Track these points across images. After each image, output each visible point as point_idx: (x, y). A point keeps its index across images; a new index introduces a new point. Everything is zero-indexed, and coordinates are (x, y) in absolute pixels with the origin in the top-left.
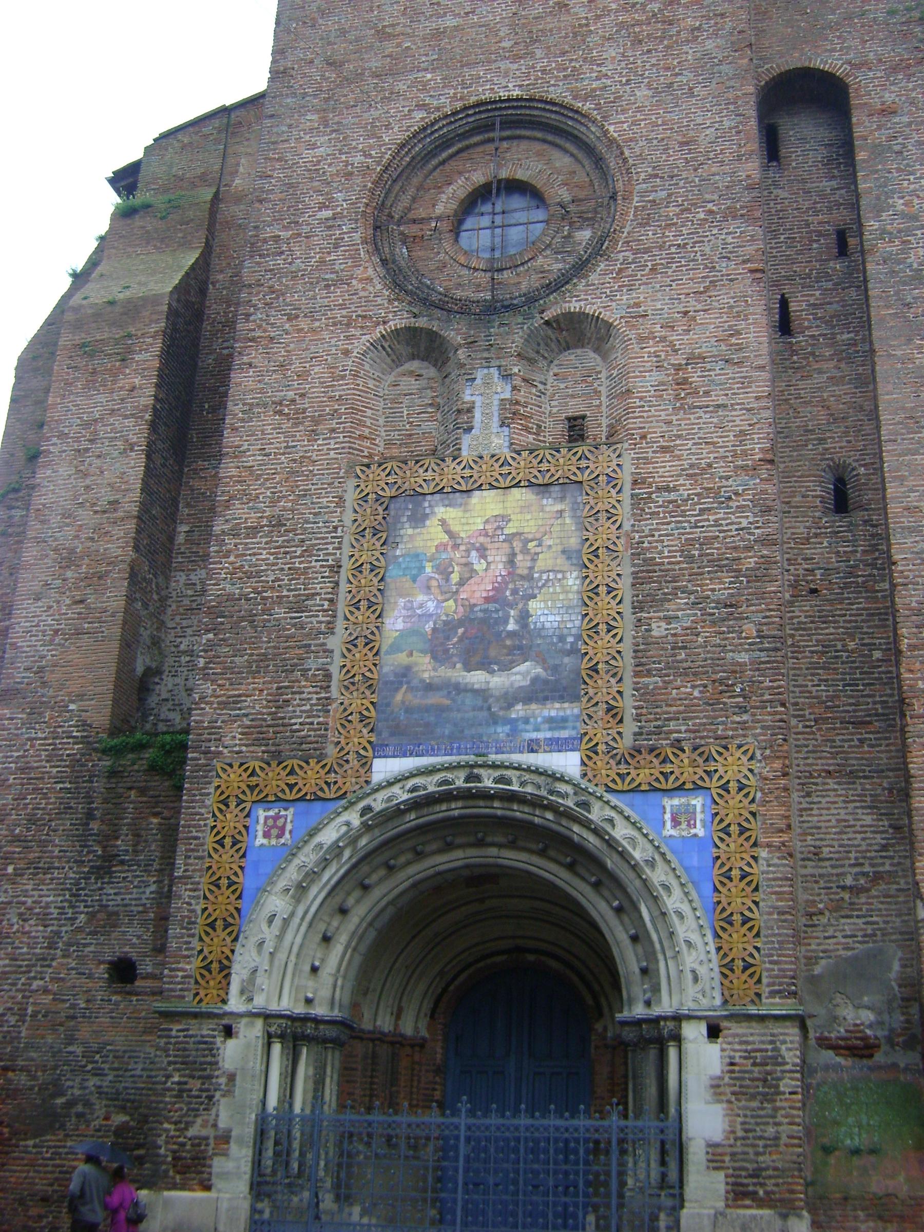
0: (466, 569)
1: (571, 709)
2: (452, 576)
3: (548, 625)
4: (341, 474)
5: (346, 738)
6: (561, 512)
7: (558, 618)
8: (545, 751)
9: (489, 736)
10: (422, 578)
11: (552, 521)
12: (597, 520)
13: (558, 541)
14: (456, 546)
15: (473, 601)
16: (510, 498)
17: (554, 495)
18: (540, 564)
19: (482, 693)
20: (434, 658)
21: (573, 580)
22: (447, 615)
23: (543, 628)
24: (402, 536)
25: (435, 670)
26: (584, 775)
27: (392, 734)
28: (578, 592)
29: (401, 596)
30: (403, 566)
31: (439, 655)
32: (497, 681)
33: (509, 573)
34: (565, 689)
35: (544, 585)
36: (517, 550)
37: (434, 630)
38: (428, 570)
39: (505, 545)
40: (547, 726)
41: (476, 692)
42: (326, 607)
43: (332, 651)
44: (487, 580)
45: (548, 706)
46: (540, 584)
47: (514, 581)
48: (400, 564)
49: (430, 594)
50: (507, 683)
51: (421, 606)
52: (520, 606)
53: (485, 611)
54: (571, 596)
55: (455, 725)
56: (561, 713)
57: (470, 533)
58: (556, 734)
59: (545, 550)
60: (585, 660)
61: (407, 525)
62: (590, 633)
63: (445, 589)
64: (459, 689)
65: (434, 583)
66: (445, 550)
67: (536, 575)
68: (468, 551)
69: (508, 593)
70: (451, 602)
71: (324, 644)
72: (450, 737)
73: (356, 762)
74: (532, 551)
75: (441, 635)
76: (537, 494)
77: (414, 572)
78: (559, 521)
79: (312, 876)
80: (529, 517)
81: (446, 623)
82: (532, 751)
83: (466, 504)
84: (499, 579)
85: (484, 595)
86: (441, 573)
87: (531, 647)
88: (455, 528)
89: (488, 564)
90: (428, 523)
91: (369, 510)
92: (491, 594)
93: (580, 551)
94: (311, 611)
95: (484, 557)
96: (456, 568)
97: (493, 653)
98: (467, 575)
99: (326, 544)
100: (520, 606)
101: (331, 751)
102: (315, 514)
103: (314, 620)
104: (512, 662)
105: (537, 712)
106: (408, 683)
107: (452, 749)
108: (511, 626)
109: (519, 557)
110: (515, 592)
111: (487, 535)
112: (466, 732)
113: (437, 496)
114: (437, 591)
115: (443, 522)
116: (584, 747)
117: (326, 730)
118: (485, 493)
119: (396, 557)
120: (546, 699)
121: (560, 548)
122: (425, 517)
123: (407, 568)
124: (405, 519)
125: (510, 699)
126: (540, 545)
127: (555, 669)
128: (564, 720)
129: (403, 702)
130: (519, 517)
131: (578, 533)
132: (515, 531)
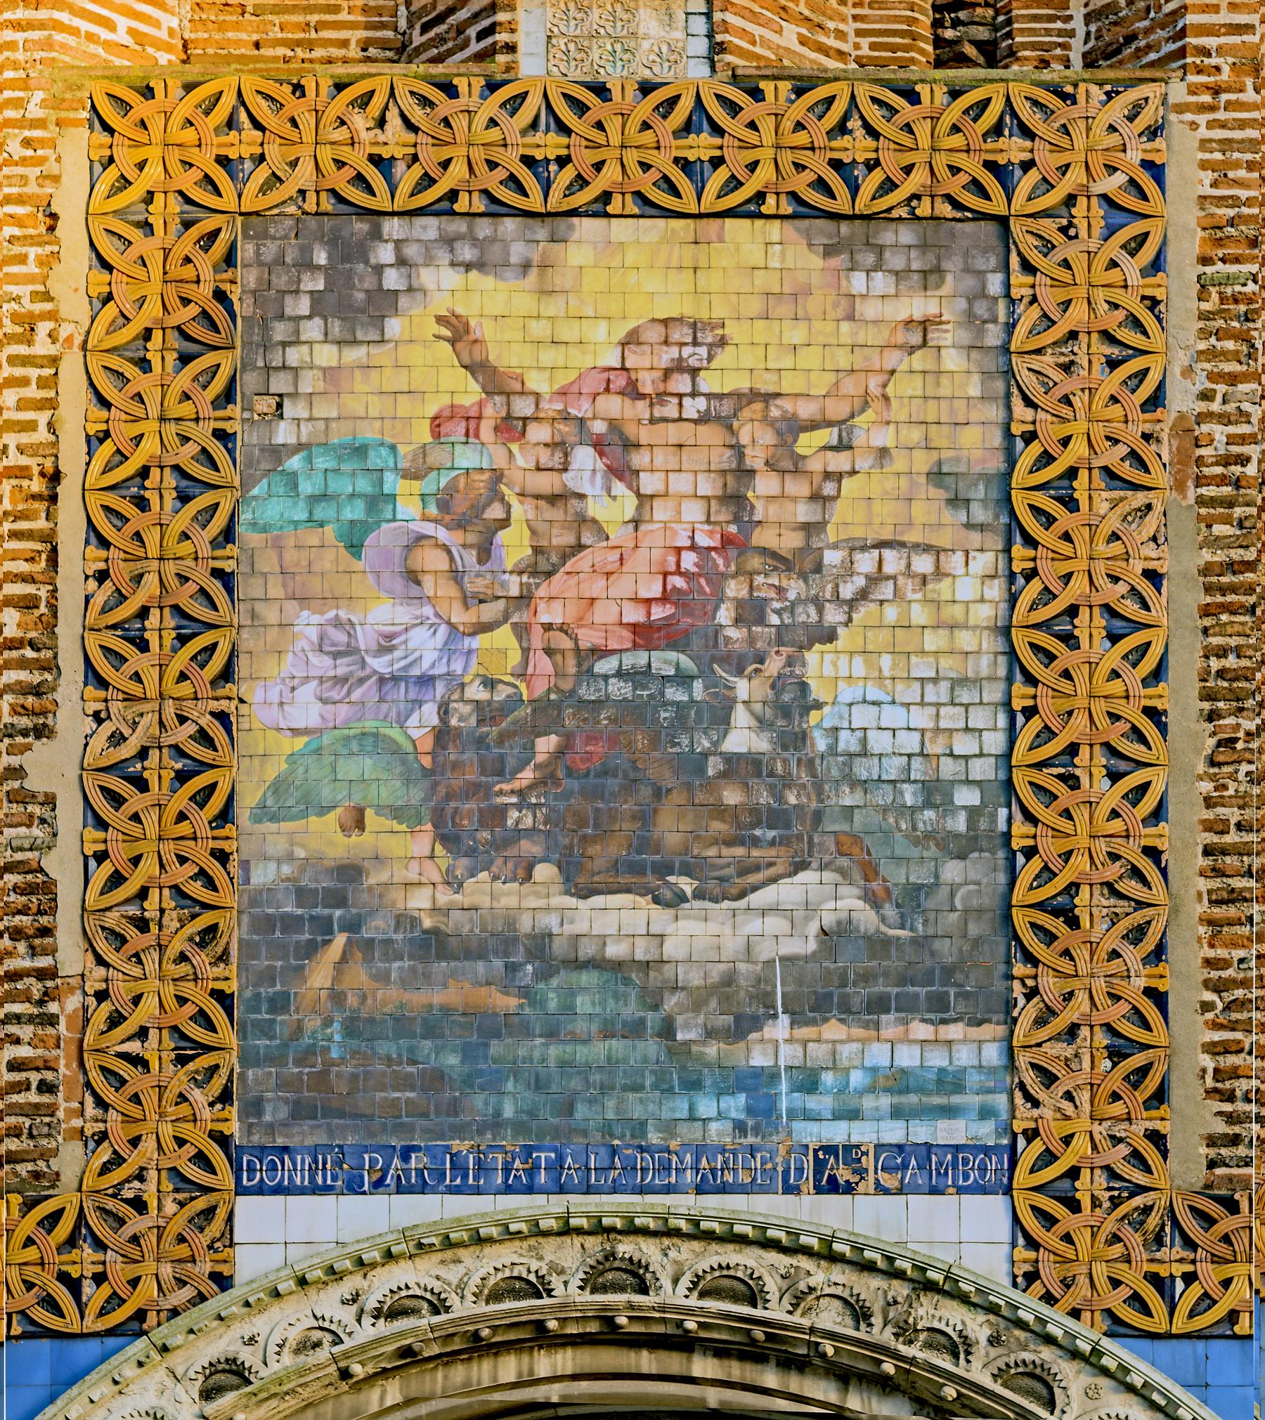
3: (879, 742)
7: (921, 718)
10: (384, 538)
11: (892, 359)
14: (511, 428)
15: (588, 638)
18: (846, 517)
21: (974, 584)
29: (303, 600)
33: (727, 541)
35: (863, 595)
36: (756, 459)
37: (442, 735)
38: (408, 508)
39: (708, 434)
44: (639, 561)
46: (847, 591)
48: (292, 481)
51: (386, 645)
52: (774, 665)
54: (966, 640)
57: (563, 379)
63: (476, 585)
65: (433, 560)
66: (471, 434)
67: (832, 558)
69: (725, 615)
70: (504, 636)
74: (815, 465)
76: (829, 251)
77: (355, 511)
78: (919, 360)
80: (797, 334)
84: (689, 561)
85: (634, 615)
88: (506, 353)
90: (394, 326)
92: (658, 612)
95: (622, 472)
98: (564, 538)
100: (774, 665)
108: (743, 737)
109: (765, 484)
110: (750, 612)
111: (633, 392)
114: (448, 590)
115: (457, 331)
119: (277, 453)
121: (923, 462)
126: (843, 446)
132: (742, 383)
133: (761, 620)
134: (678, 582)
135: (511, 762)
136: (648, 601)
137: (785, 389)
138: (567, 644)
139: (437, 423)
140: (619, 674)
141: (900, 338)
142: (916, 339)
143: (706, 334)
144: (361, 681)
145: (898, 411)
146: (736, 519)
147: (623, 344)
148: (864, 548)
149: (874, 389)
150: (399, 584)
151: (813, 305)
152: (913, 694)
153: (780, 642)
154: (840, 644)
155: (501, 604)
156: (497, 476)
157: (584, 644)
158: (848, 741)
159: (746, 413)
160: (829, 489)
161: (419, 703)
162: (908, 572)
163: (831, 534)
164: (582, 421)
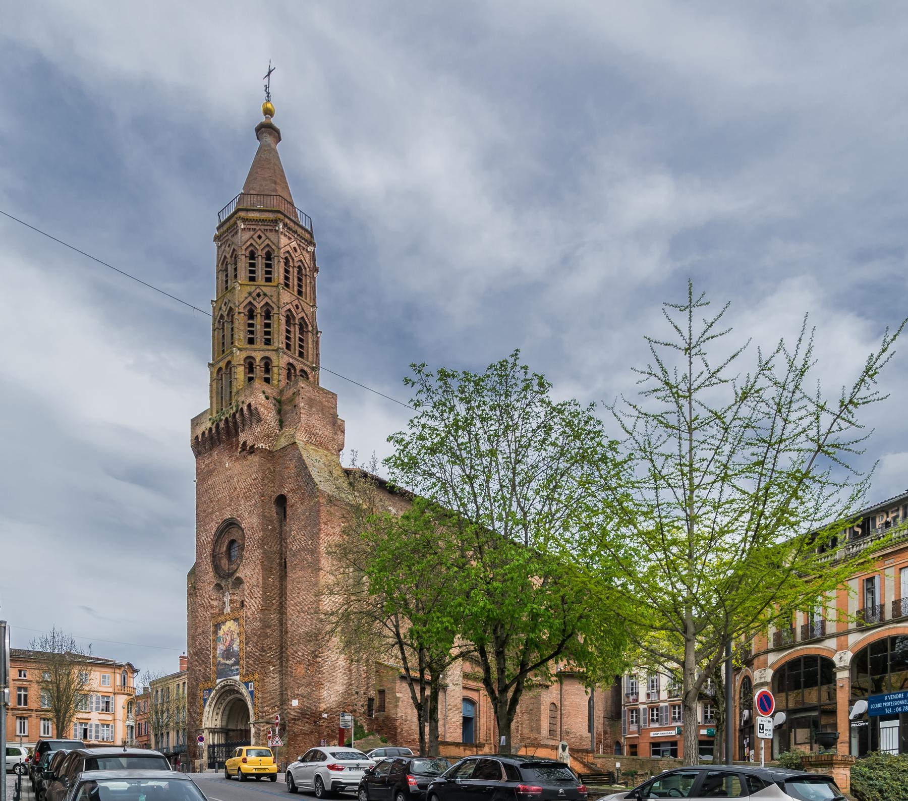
64: (226, 664)
79: (211, 703)
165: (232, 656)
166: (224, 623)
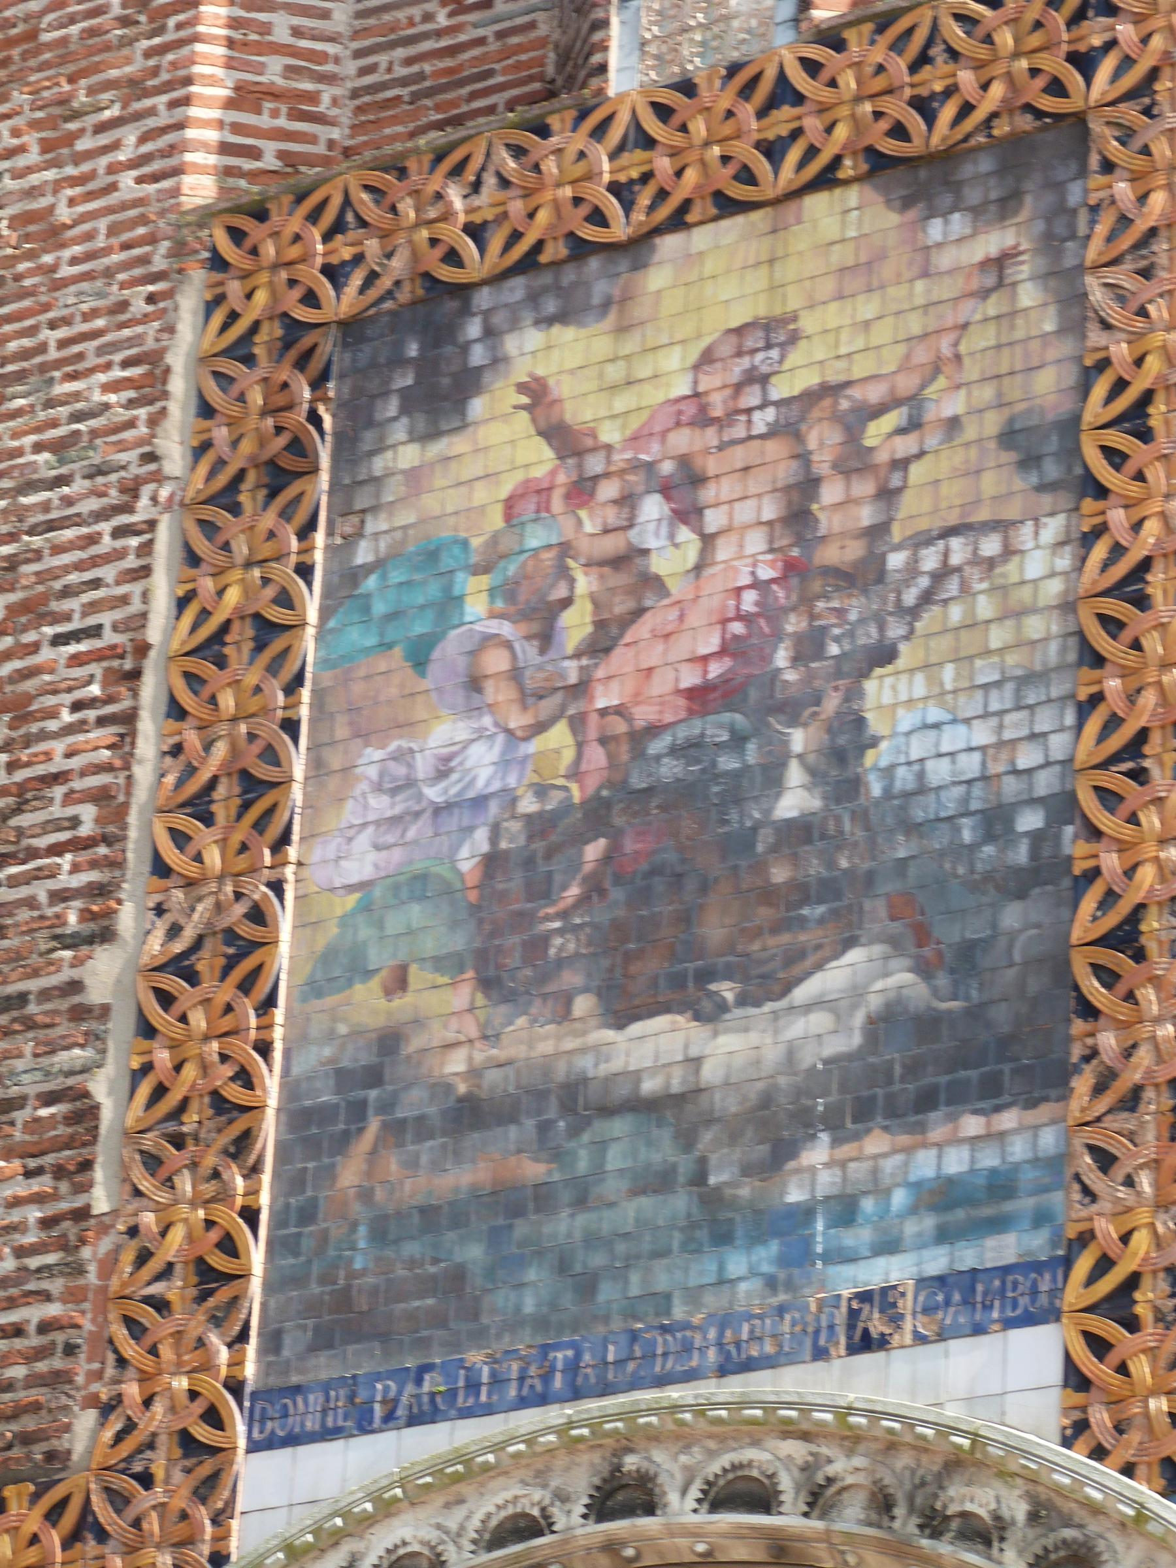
0: (621, 579)
1: (1022, 1136)
2: (568, 618)
3: (939, 772)
4: (159, 263)
5: (145, 1378)
6: (1000, 263)
7: (982, 734)
8: (920, 1339)
9: (693, 1296)
10: (451, 648)
12: (1146, 273)
13: (987, 393)
14: (581, 491)
15: (644, 715)
16: (799, 240)
17: (973, 196)
18: (915, 509)
19: (675, 1109)
20: (487, 984)
21: (1043, 559)
22: (541, 791)
23: (922, 788)
24: (376, 481)
25: (489, 1037)
26: (1075, 1430)
27: (323, 1341)
28: (1068, 606)
29: (364, 735)
30: (379, 608)
31: (502, 970)
32: (732, 1050)
33: (792, 569)
34: (1005, 1043)
35: (927, 598)
36: (822, 462)
37: (492, 862)
38: (476, 607)
39: (775, 449)
40: (929, 1222)
41: (648, 1108)
42: (86, 829)
43: (105, 1011)
44: (695, 618)
45: (936, 1134)
46: (910, 597)
47: (806, 602)
49: (474, 711)
50: (772, 1055)
51: (442, 773)
52: (832, 704)
53: (683, 750)
54: (1035, 626)
55: (563, 1267)
56: (989, 1159)
57: (635, 423)
58: (968, 1256)
59: (932, 440)
60: (1089, 904)
61: (399, 431)
62: (1113, 779)
63: (532, 681)
64: (581, 1103)
65: (496, 662)
66: (544, 507)
67: (896, 560)
68: (628, 501)
69: (782, 657)
70: (559, 736)
71: (75, 986)
72: (541, 1323)
73: (178, 1476)
74: (882, 457)
75: (514, 882)
76: (907, 203)
77: (420, 627)
78: (993, 306)
80: (867, 308)
81: (538, 825)
82: (865, 1343)
83: (626, 299)
84: (749, 601)
85: (690, 678)
86: (521, 616)
87: (870, 879)
88: (581, 408)
89: (708, 540)
90: (477, 406)
91: (257, 398)
92: (715, 670)
93: (1071, 426)
94: (33, 854)
95: (688, 514)
96: (584, 583)
97: (714, 930)
98: (621, 605)
99: (95, 562)
100: (832, 704)
101: (84, 1433)
102: (58, 447)
103: (40, 891)
104: (794, 956)
105: (889, 1165)
106: (385, 1107)
107: (547, 1378)
108: (795, 799)
109: (831, 493)
110: (809, 647)
111: (703, 420)
112: (607, 1292)
113: (517, 288)
115: (537, 394)
116: (1075, 1293)
117: (70, 1350)
118: (701, 238)
119: (354, 576)
120: (927, 1101)
121: (993, 423)
122: (469, 383)
123: (392, 616)
124: (392, 407)
125: (775, 1125)
126: (913, 425)
127: (967, 960)
128: (1001, 1185)
129: (365, 1195)
130: (832, 315)
131: (1066, 347)
132: (807, 380)
133: (819, 652)
134: (737, 628)
135: (558, 878)
136: (705, 659)
137: (858, 373)
138: (620, 727)
139: (510, 505)
140: (674, 751)
141: (975, 284)
142: (990, 280)
143: (777, 331)
144: (417, 815)
145: (971, 370)
146: (800, 540)
147: (696, 367)
148: (929, 542)
149: (946, 350)
150: (460, 697)
151: (887, 270)
152: (970, 706)
153: (838, 674)
154: (901, 663)
155: (558, 698)
156: (565, 549)
157: (640, 724)
158: (904, 778)
159: (816, 413)
160: (896, 481)
161: (470, 829)
162: (976, 560)
163: (897, 533)
164: (650, 467)
165: (838, 908)
166: (575, 267)
